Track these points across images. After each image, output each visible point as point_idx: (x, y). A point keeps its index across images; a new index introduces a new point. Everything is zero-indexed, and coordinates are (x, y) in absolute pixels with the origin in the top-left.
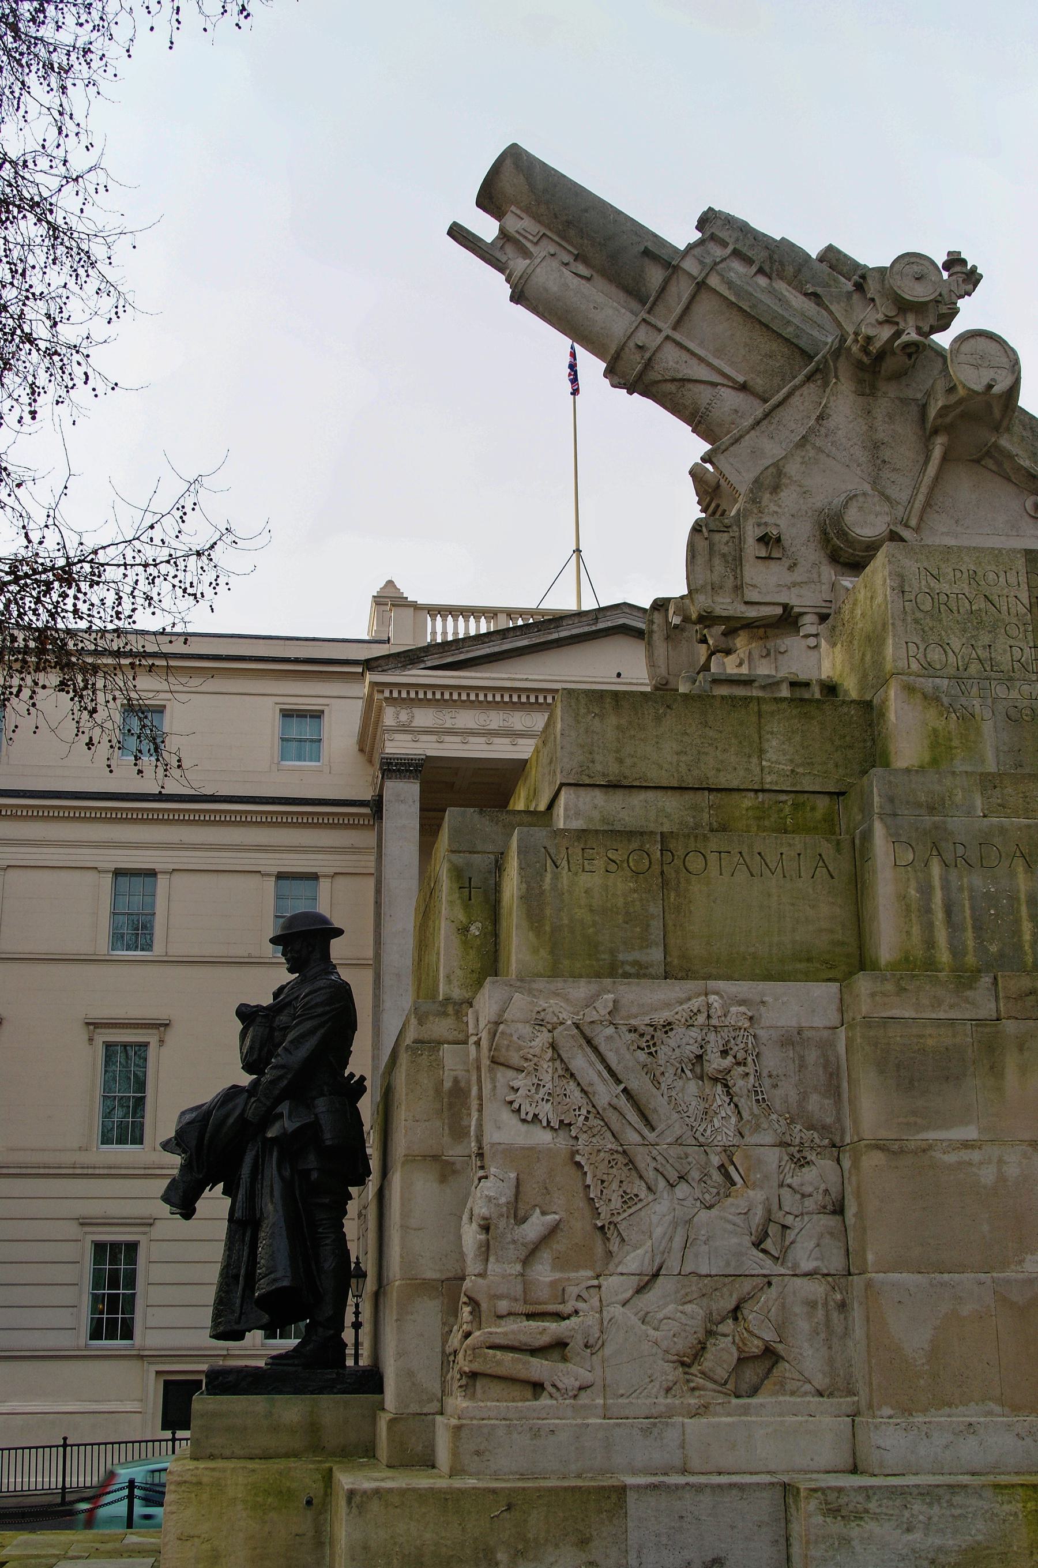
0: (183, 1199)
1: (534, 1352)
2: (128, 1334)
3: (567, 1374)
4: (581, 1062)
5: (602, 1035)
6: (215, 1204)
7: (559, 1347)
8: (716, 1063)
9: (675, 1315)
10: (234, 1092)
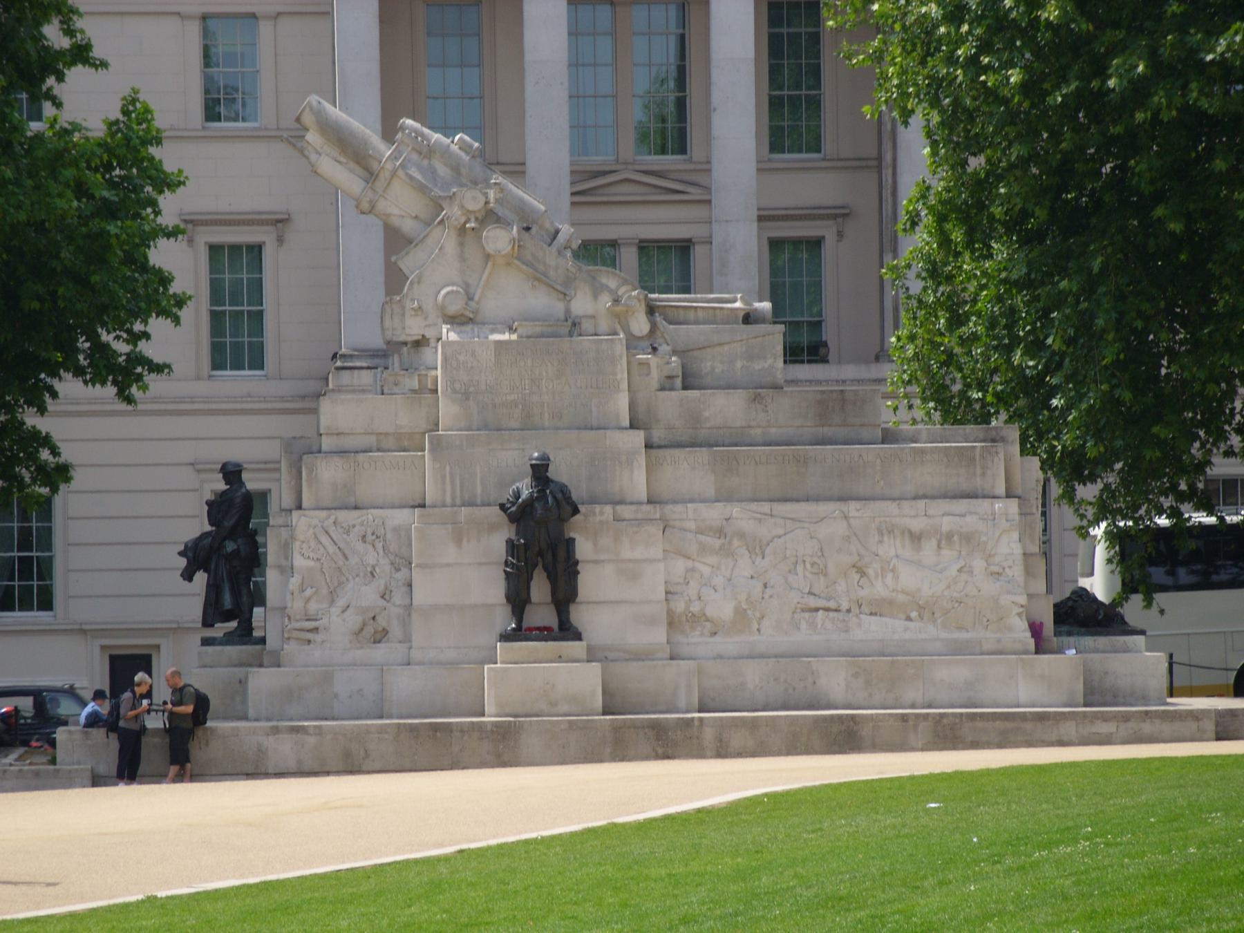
0: (188, 575)
1: (309, 631)
2: (46, 603)
3: (318, 638)
4: (325, 539)
5: (332, 530)
6: (201, 578)
7: (316, 630)
8: (370, 538)
9: (353, 619)
10: (204, 535)
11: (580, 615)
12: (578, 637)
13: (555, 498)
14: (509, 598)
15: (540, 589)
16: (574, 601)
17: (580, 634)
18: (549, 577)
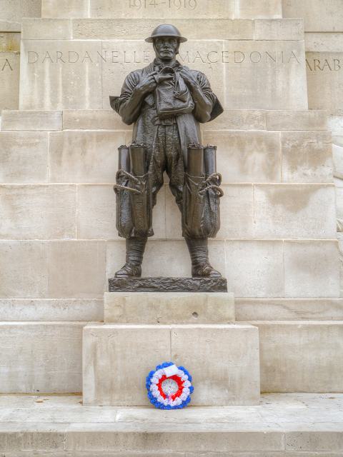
11: (221, 256)
12: (221, 286)
13: (187, 83)
14: (122, 230)
15: (166, 219)
16: (213, 235)
17: (224, 281)
18: (178, 200)
